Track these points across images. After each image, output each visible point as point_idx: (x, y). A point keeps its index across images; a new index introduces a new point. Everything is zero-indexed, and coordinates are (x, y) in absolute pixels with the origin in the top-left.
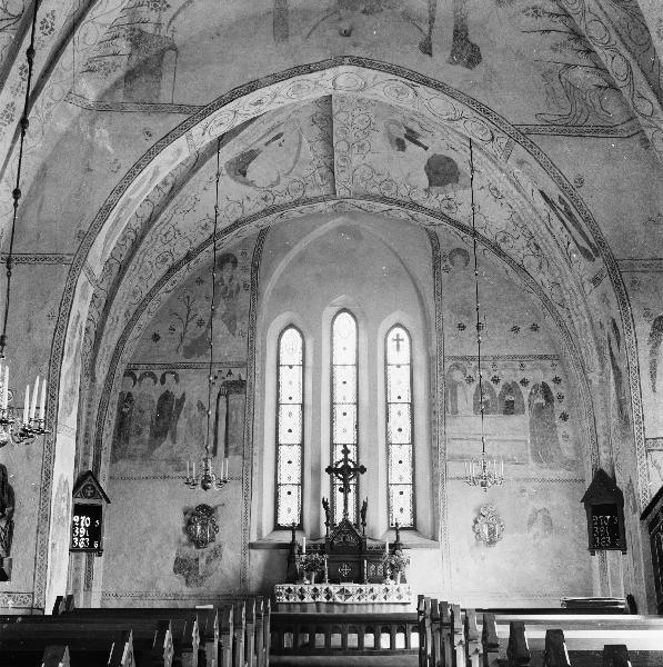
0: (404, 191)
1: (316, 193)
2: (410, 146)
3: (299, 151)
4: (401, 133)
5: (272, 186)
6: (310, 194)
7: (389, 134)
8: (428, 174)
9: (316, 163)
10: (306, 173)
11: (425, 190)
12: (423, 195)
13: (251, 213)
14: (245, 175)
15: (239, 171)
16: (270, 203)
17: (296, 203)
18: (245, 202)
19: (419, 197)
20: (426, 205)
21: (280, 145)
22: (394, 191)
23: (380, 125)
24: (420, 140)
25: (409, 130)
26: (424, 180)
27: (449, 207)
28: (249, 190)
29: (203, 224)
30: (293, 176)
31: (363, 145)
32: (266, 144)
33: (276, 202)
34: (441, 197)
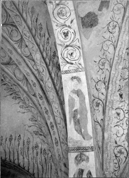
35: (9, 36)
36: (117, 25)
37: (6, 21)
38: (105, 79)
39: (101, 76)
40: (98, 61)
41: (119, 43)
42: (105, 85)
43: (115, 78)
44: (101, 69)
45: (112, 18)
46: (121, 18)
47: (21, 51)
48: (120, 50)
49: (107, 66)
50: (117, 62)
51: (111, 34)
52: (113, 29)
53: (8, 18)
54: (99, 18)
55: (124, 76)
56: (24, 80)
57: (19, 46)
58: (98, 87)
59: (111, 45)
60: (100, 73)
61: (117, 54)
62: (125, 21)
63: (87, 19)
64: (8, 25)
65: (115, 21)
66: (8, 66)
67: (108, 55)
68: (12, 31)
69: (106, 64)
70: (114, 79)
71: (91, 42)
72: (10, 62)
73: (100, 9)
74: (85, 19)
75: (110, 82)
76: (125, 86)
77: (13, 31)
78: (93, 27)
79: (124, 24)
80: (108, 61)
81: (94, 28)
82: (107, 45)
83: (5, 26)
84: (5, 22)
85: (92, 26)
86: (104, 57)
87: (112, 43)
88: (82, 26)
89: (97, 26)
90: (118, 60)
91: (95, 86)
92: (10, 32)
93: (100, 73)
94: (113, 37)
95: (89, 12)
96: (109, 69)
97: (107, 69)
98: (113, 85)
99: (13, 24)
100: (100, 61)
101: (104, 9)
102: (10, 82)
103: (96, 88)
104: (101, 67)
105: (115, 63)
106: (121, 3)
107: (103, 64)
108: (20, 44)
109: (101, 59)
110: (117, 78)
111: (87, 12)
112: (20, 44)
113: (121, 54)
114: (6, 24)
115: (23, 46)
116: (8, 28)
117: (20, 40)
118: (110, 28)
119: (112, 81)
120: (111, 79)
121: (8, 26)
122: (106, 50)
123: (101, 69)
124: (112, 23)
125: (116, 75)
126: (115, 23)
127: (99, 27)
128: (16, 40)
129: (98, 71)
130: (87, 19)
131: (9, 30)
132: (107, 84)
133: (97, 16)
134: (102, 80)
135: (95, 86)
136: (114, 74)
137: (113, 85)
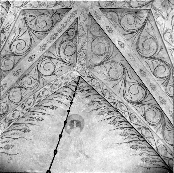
35: (152, 71)
37: (153, 55)
47: (166, 90)
53: (157, 53)
56: (160, 125)
57: (163, 83)
64: (155, 59)
66: (138, 105)
68: (157, 66)
72: (142, 101)
77: (160, 67)
83: (151, 59)
84: (152, 56)
92: (156, 67)
99: (162, 59)
102: (139, 124)
108: (166, 81)
112: (166, 81)
114: (151, 58)
115: (169, 85)
116: (154, 62)
117: (166, 78)
121: (154, 60)
128: (162, 77)
131: (154, 64)
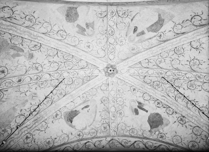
0: (140, 133)
1: (102, 135)
2: (140, 111)
3: (95, 116)
4: (136, 106)
5: (83, 130)
6: (99, 135)
7: (131, 107)
8: (149, 123)
9: (102, 122)
10: (98, 126)
11: (149, 131)
12: (149, 133)
13: (72, 140)
14: (71, 122)
15: (69, 119)
16: (81, 137)
17: (93, 138)
18: (70, 135)
19: (147, 134)
20: (151, 137)
21: (88, 112)
22: (135, 133)
23: (127, 103)
24: (144, 107)
25: (140, 103)
26: (148, 127)
27: (162, 137)
28: (72, 130)
29: (48, 141)
30: (92, 126)
31: (121, 113)
32: (82, 109)
33: (84, 137)
34: (157, 133)
36: (63, 39)
38: (14, 18)
39: (18, 16)
40: (35, 15)
41: (49, 38)
42: (8, 18)
43: (16, 30)
44: (26, 17)
45: (69, 35)
46: (68, 43)
48: (43, 38)
49: (28, 23)
50: (31, 34)
51: (56, 32)
52: (60, 34)
54: (72, 23)
55: (15, 39)
58: (6, 9)
59: (47, 31)
60: (21, 15)
61: (40, 35)
62: (66, 45)
63: (74, 12)
65: (67, 37)
67: (38, 27)
69: (29, 22)
70: (15, 28)
71: (54, 12)
73: (78, 26)
74: (74, 10)
75: (12, 24)
76: (3, 39)
78: (66, 16)
79: (65, 44)
80: (33, 26)
81: (64, 17)
82: (48, 27)
85: (67, 16)
86: (37, 23)
87: (48, 32)
88: (70, 7)
89: (65, 20)
90: (34, 35)
91: (8, 7)
93: (21, 15)
94: (54, 33)
95: (78, 16)
96: (25, 25)
97: (24, 23)
98: (8, 26)
100: (34, 17)
101: (77, 29)
103: (5, 7)
104: (27, 17)
105: (31, 32)
106: (79, 43)
107: (30, 20)
109: (36, 18)
110: (16, 31)
111: (79, 14)
113: (39, 38)
118: (62, 31)
119: (12, 26)
120: (14, 25)
122: (43, 25)
123: (26, 17)
124: (65, 34)
125: (18, 31)
126: (64, 37)
127: (65, 22)
129: (24, 13)
130: (74, 12)
132: (8, 20)
133: (74, 22)
134: (13, 15)
135: (8, 7)
136: (20, 30)
137: (8, 26)
